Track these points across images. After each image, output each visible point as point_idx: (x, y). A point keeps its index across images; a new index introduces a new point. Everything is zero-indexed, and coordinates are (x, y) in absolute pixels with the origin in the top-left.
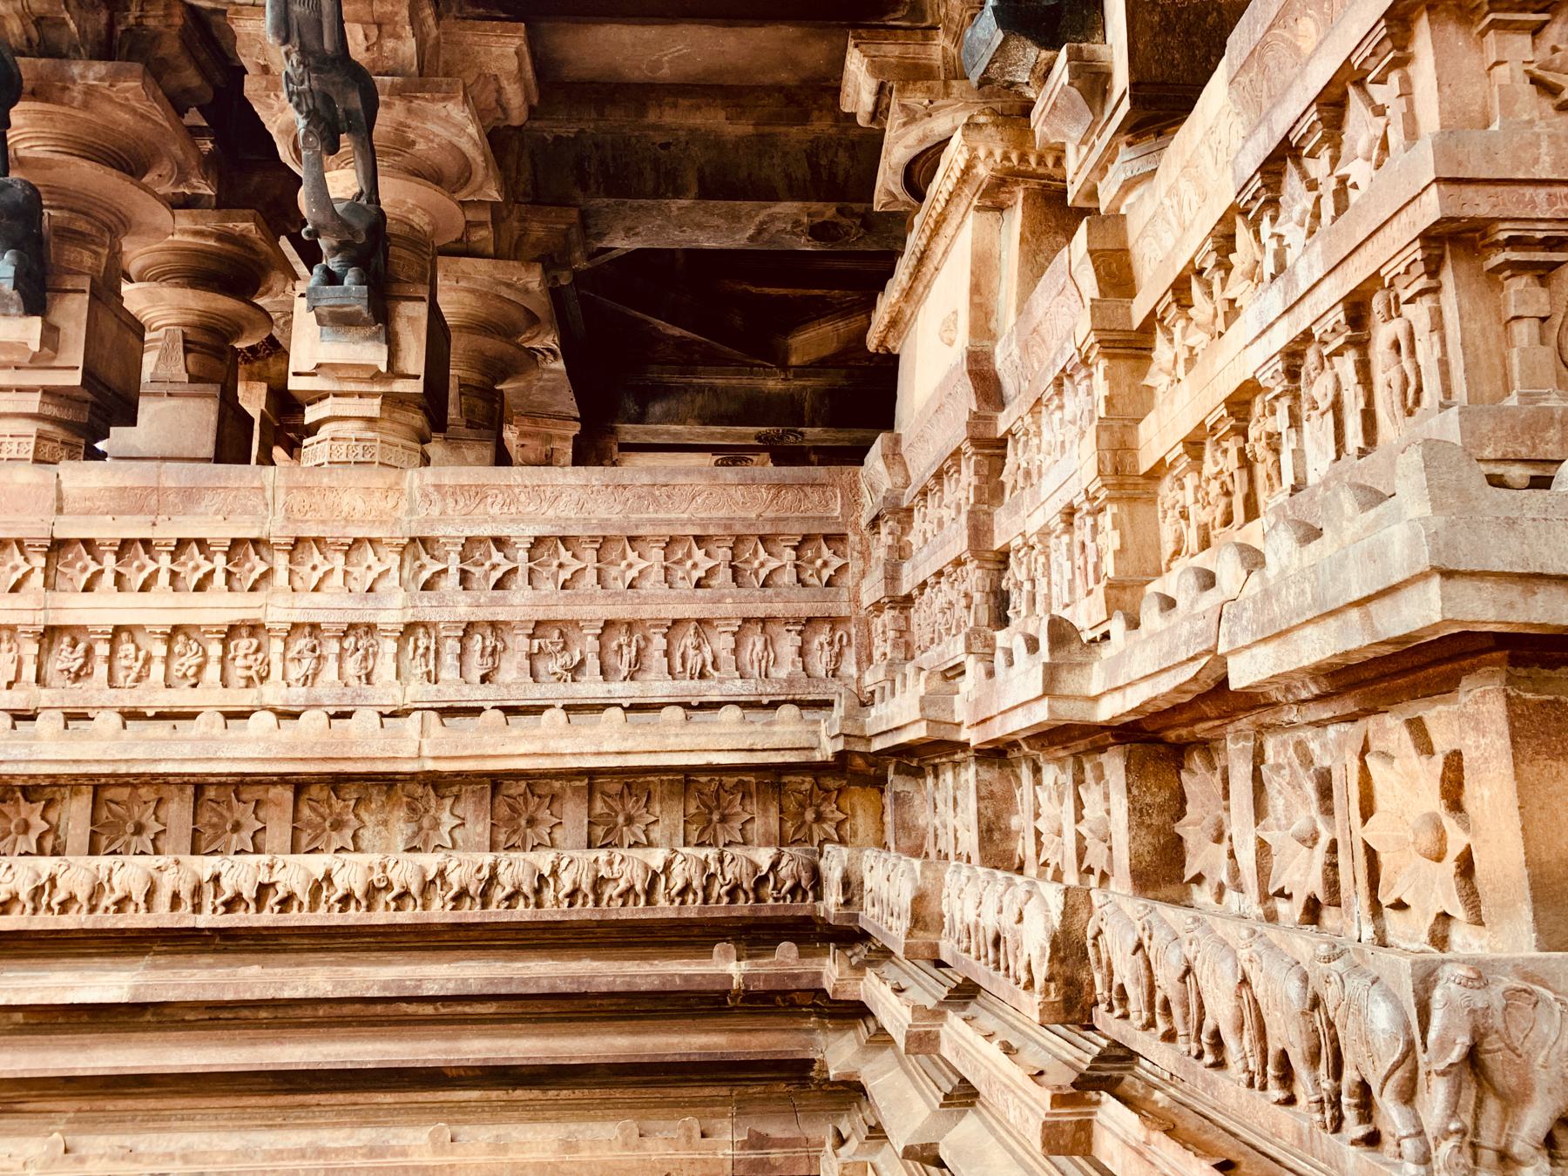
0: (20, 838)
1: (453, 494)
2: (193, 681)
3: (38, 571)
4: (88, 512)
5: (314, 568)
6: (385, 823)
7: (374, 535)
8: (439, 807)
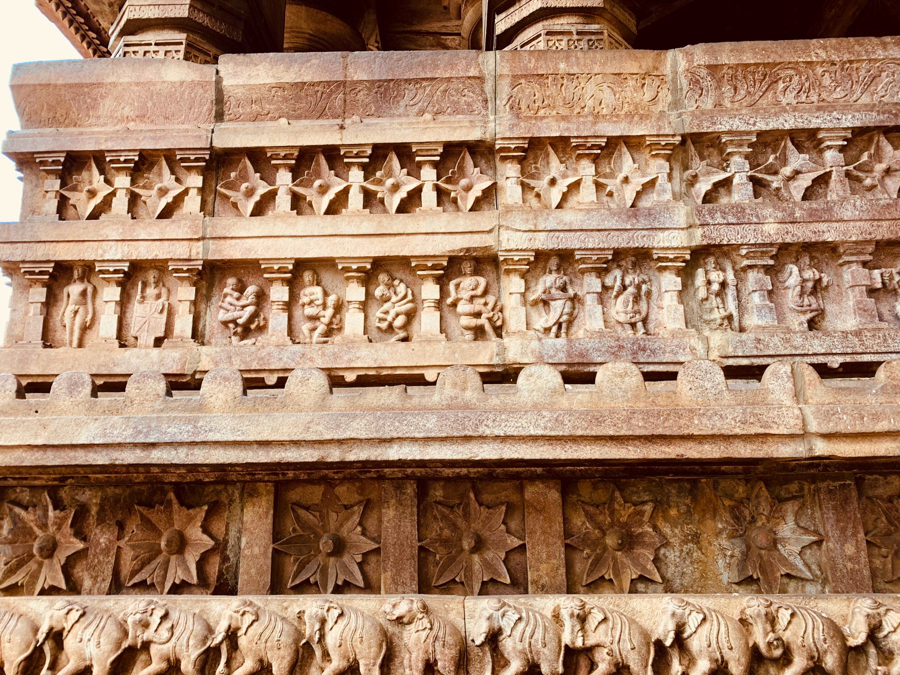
0: (173, 558)
1: (734, 77)
2: (402, 334)
3: (193, 193)
4: (256, 118)
5: (553, 182)
6: (696, 538)
7: (637, 131)
8: (776, 515)
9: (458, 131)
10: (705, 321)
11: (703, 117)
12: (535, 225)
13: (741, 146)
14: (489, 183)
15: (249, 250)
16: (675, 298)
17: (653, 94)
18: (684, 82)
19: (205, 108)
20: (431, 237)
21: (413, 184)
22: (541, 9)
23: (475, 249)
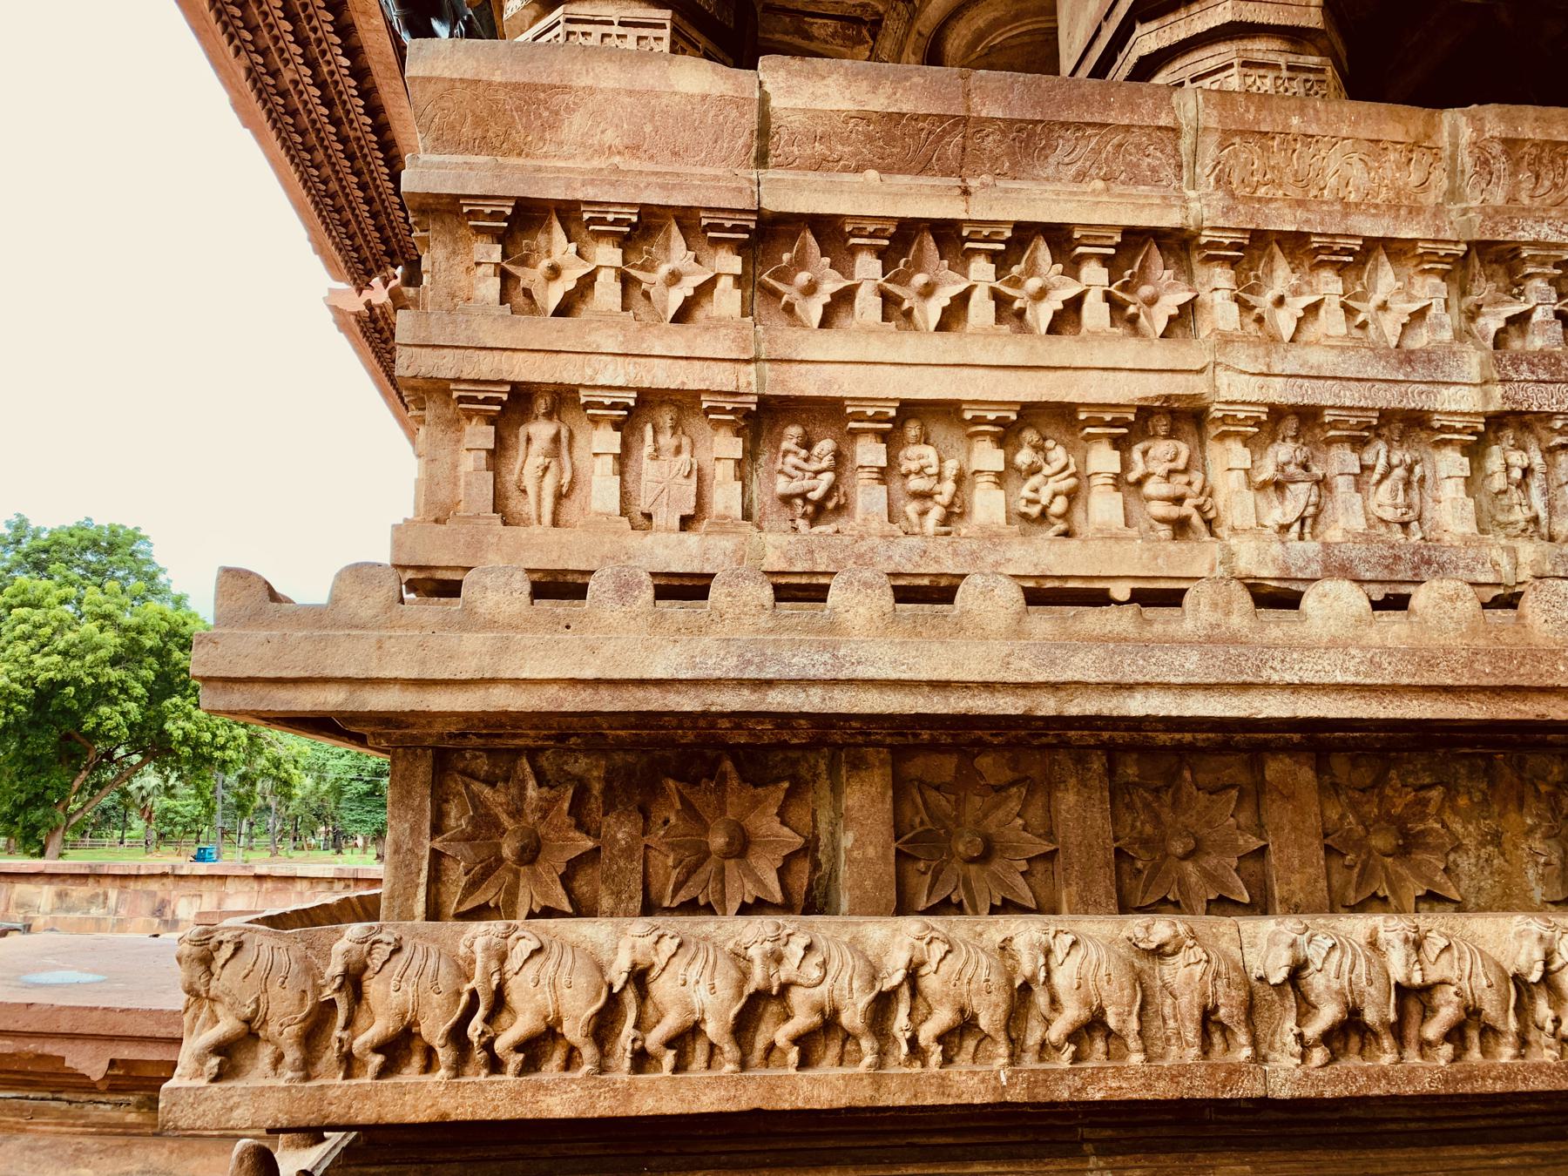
0: (730, 864)
2: (1061, 526)
3: (725, 283)
4: (819, 165)
9: (1147, 211)
10: (1499, 524)
11: (1498, 218)
12: (1269, 366)
13: (1543, 264)
14: (1188, 296)
15: (830, 383)
16: (1462, 488)
17: (1423, 175)
18: (1466, 160)
19: (741, 142)
20: (1111, 374)
21: (1070, 290)
22: (1231, 23)
23: (1178, 397)
